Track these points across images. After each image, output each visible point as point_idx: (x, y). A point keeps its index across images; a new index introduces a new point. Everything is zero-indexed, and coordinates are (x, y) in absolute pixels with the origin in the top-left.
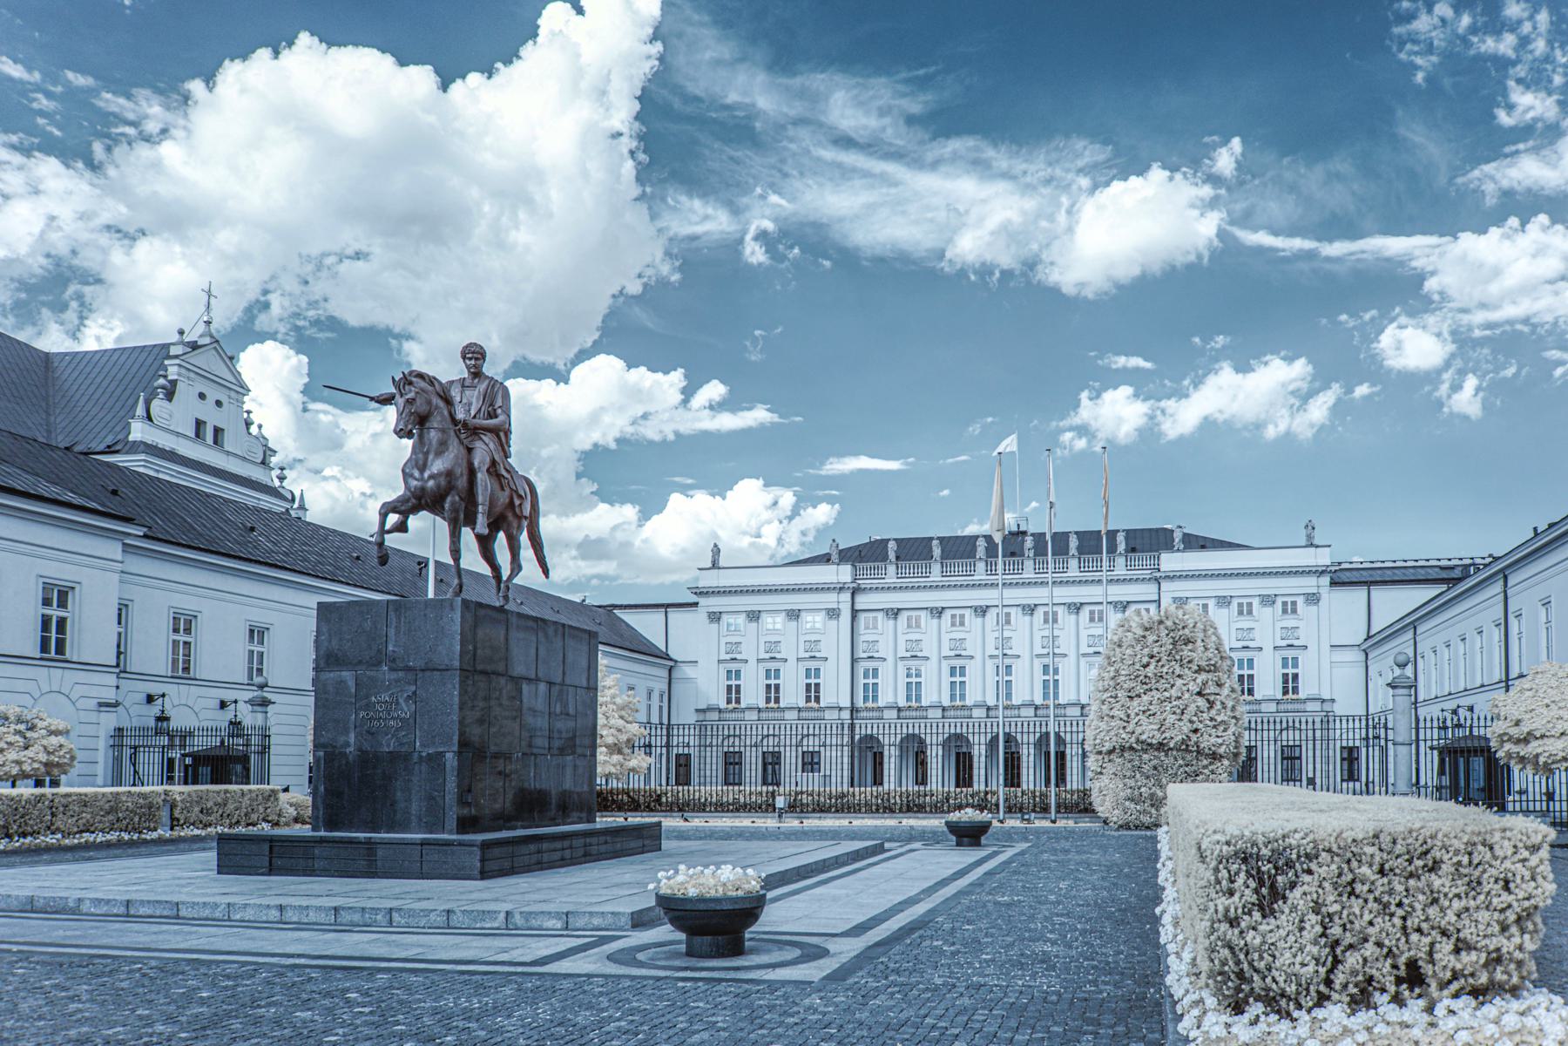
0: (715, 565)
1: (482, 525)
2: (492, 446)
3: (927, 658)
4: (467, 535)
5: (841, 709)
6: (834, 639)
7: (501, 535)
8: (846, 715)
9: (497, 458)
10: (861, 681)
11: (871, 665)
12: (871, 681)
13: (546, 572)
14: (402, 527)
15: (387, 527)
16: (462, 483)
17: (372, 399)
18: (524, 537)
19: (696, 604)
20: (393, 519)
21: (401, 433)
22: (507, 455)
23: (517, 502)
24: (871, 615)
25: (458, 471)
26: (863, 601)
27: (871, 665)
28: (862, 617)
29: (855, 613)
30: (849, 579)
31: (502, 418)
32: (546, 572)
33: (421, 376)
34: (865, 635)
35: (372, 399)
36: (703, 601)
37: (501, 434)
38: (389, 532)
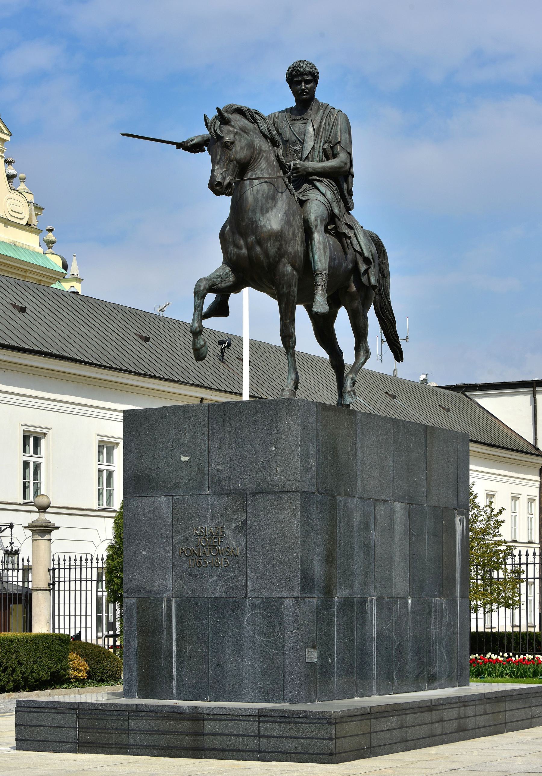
1: (321, 304)
2: (329, 195)
4: (300, 310)
7: (343, 314)
9: (336, 211)
13: (399, 356)
14: (221, 309)
15: (205, 309)
16: (296, 247)
17: (179, 146)
18: (371, 314)
20: (210, 298)
21: (217, 188)
22: (348, 208)
23: (363, 267)
25: (289, 232)
31: (343, 156)
32: (399, 356)
33: (240, 111)
35: (179, 146)
37: (341, 178)
38: (207, 316)
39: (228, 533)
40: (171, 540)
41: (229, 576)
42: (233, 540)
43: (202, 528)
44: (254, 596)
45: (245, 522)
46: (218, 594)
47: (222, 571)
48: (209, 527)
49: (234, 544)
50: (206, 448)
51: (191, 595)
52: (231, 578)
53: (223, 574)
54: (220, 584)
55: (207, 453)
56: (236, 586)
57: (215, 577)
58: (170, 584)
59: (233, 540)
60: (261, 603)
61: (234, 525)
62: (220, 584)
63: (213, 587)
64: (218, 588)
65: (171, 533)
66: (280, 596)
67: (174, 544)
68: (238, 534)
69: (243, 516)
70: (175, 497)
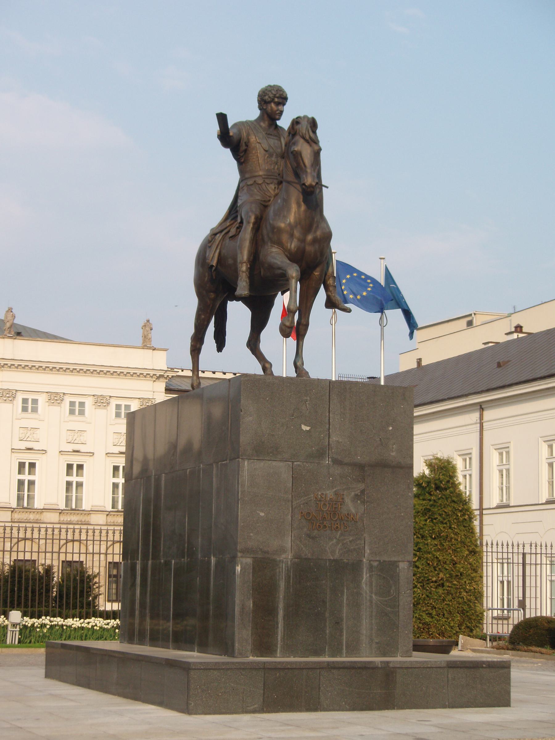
3: (45, 451)
39: (348, 501)
40: (290, 503)
41: (348, 540)
43: (323, 494)
44: (372, 558)
45: (363, 492)
46: (337, 556)
47: (342, 534)
48: (330, 494)
49: (353, 511)
50: (327, 421)
51: (309, 556)
52: (350, 542)
53: (342, 538)
54: (339, 546)
55: (328, 426)
56: (355, 549)
57: (335, 541)
58: (288, 542)
59: (350, 506)
60: (378, 565)
61: (353, 493)
62: (339, 546)
63: (332, 548)
64: (337, 551)
65: (290, 496)
66: (396, 559)
67: (293, 507)
68: (357, 502)
69: (361, 486)
70: (295, 463)
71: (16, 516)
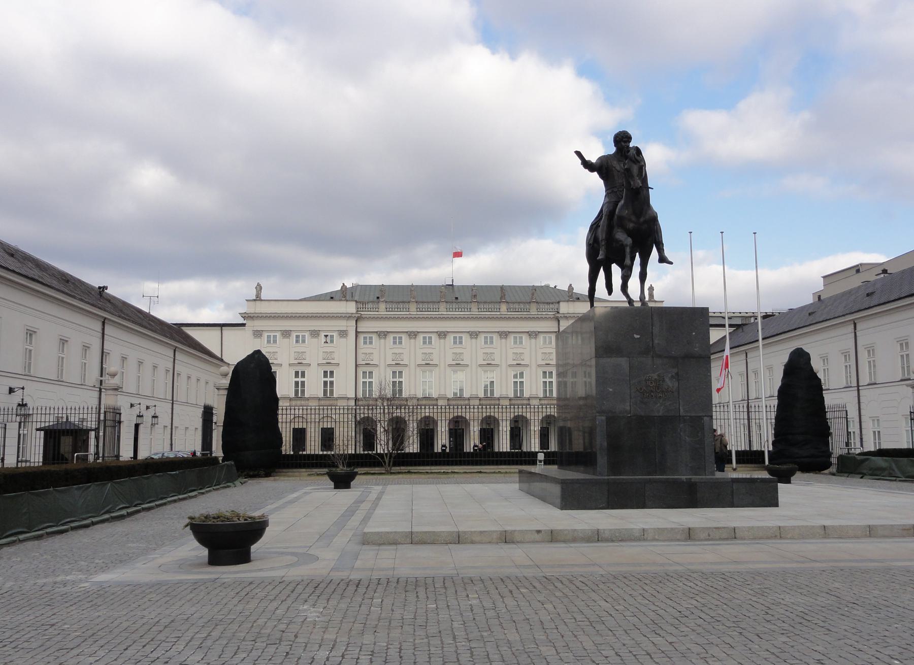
0: (258, 298)
5: (348, 399)
6: (343, 350)
8: (352, 403)
10: (361, 380)
11: (368, 369)
12: (368, 380)
19: (244, 325)
24: (368, 336)
26: (364, 326)
27: (368, 369)
28: (361, 337)
29: (357, 332)
30: (354, 311)
34: (364, 348)
36: (249, 323)
42: (670, 383)
71: (322, 402)
